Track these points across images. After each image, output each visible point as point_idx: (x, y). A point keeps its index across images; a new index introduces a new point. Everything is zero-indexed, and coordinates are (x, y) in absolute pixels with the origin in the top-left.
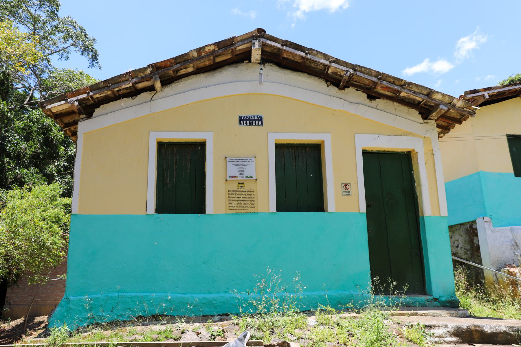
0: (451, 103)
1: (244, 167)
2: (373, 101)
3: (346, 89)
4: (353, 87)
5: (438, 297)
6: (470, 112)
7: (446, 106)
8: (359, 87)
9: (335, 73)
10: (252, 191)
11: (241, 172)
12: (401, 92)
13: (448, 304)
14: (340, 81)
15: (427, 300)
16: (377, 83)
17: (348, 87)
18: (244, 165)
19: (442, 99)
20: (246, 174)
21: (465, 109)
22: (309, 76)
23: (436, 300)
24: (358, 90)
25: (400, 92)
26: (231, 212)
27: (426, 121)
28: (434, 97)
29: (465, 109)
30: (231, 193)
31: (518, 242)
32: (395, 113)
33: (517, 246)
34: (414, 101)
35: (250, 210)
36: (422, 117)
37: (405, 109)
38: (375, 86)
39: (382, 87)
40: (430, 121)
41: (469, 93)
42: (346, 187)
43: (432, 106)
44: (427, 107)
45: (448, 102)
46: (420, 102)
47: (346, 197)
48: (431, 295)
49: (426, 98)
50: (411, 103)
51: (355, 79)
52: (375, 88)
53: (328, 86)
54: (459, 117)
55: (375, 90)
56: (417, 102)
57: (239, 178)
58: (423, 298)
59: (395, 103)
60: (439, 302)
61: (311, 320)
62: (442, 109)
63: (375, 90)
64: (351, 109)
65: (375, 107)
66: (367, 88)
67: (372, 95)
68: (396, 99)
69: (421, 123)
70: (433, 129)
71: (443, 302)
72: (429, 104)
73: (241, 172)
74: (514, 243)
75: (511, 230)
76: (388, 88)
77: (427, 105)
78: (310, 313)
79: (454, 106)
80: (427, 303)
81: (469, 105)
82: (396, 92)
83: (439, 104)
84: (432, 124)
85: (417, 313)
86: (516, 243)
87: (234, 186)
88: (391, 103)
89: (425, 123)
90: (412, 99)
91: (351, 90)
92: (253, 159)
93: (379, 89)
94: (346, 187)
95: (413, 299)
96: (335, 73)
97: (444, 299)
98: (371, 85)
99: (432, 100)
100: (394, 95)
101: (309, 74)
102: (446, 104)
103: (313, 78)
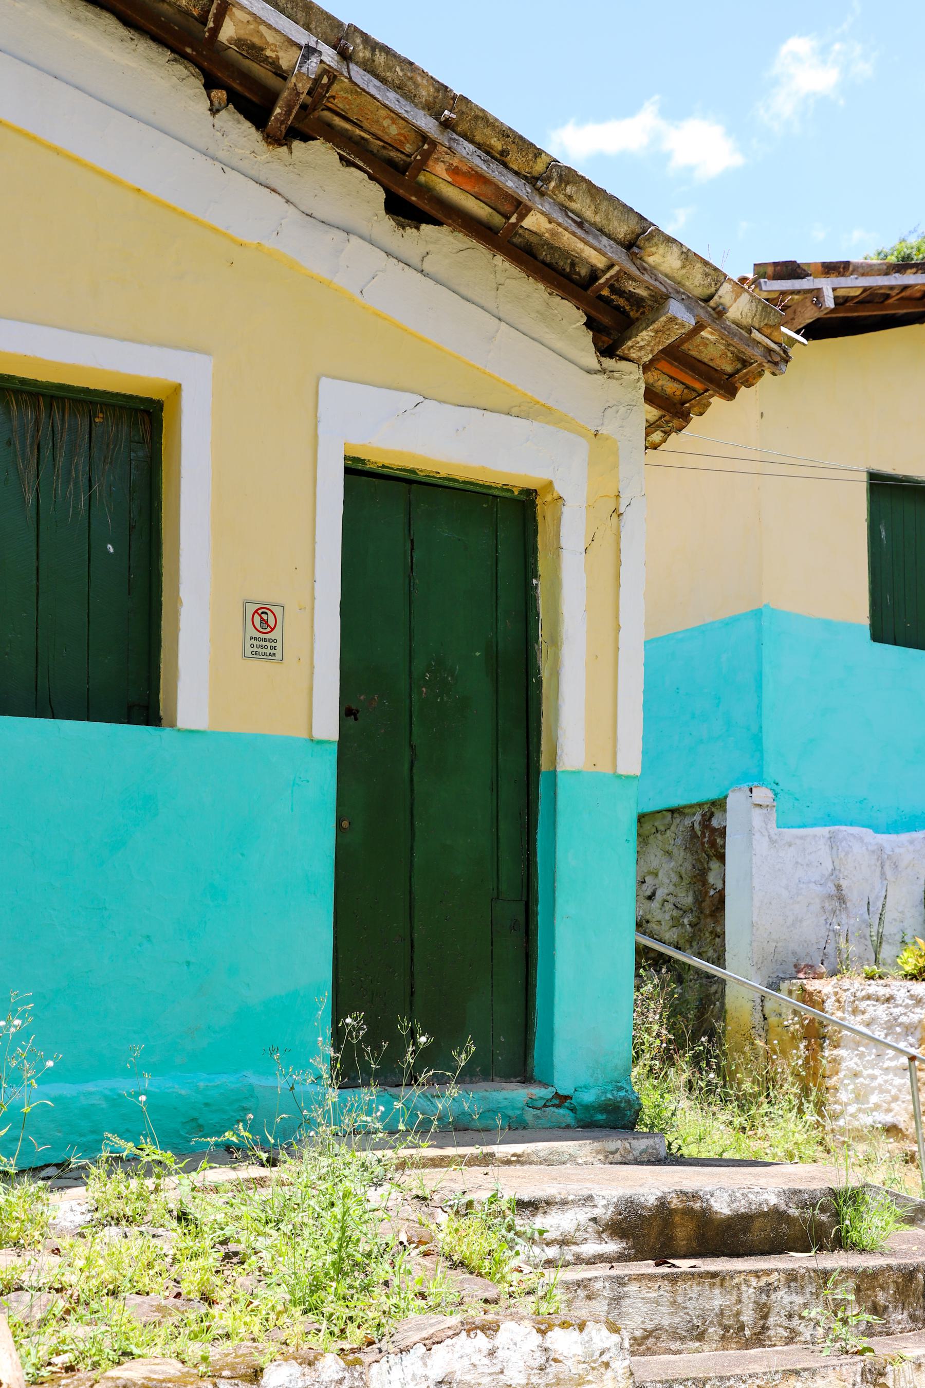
0: (711, 297)
2: (411, 232)
3: (297, 144)
4: (328, 140)
6: (770, 350)
7: (690, 309)
8: (358, 151)
9: (254, 51)
12: (529, 210)
13: (600, 1117)
14: (272, 97)
15: (531, 1104)
16: (434, 144)
17: (306, 138)
19: (679, 275)
21: (756, 335)
22: (123, 31)
23: (562, 1099)
24: (350, 164)
25: (522, 208)
27: (609, 363)
28: (651, 260)
29: (756, 335)
31: (844, 884)
32: (491, 305)
33: (842, 899)
34: (573, 265)
36: (595, 342)
37: (535, 292)
38: (427, 156)
39: (454, 171)
40: (623, 365)
41: (770, 270)
43: (636, 301)
44: (621, 302)
45: (698, 292)
46: (594, 275)
48: (546, 1085)
49: (619, 256)
50: (561, 273)
51: (339, 104)
52: (422, 166)
53: (214, 111)
54: (729, 369)
55: (422, 178)
56: (584, 271)
58: (515, 1095)
59: (499, 258)
60: (573, 1110)
61: (68, 1207)
62: (673, 320)
63: (422, 178)
64: (312, 252)
65: (415, 261)
66: (390, 162)
67: (410, 206)
68: (503, 238)
69: (589, 372)
70: (631, 406)
71: (587, 1108)
72: (630, 286)
74: (833, 891)
75: (832, 840)
76: (479, 177)
77: (621, 293)
78: (61, 1173)
79: (720, 313)
80: (530, 1115)
81: (773, 320)
82: (507, 208)
83: (667, 297)
84: (629, 380)
85: (492, 1155)
86: (839, 887)
88: (481, 252)
89: (603, 371)
90: (565, 254)
91: (318, 153)
93: (438, 178)
95: (484, 1099)
96: (253, 46)
97: (588, 1097)
98: (408, 148)
99: (643, 270)
100: (498, 220)
101: (127, 22)
102: (690, 301)
103: (144, 47)
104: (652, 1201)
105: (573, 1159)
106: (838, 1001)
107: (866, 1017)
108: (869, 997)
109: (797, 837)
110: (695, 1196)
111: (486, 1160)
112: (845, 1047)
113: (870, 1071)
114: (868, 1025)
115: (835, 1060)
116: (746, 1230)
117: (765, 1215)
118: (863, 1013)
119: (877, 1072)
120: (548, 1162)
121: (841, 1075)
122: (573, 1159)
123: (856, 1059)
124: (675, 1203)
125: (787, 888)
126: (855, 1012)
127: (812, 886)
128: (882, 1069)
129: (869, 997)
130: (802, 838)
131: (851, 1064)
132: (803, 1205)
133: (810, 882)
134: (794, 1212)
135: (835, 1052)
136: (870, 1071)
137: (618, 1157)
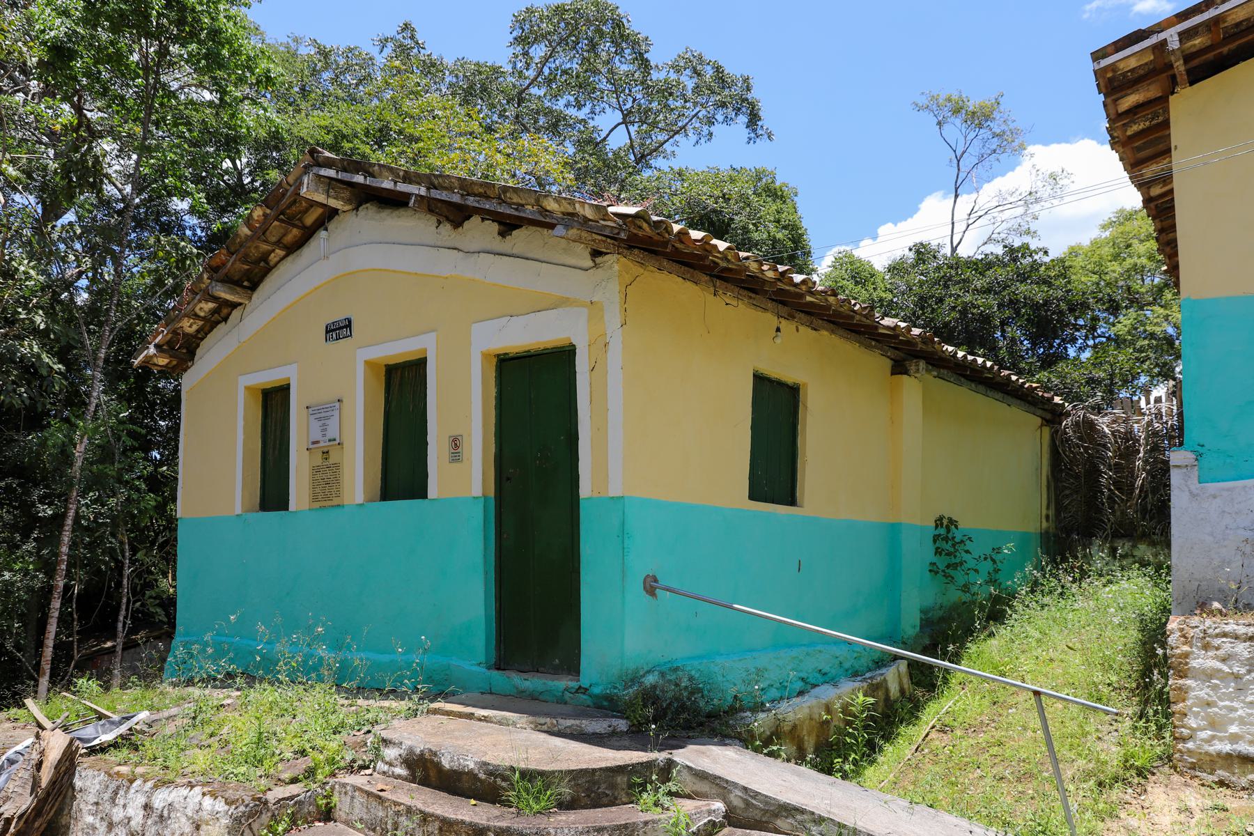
1: (327, 422)
5: (587, 686)
8: (487, 215)
10: (337, 466)
11: (324, 430)
13: (605, 703)
18: (327, 418)
20: (330, 435)
26: (317, 505)
30: (316, 470)
35: (336, 501)
42: (456, 443)
47: (454, 465)
57: (322, 444)
58: (562, 683)
71: (597, 696)
73: (324, 430)
80: (568, 695)
87: (318, 460)
92: (337, 404)
94: (456, 443)
97: (597, 690)
104: (418, 751)
105: (514, 724)
106: (1184, 636)
107: (1221, 652)
108: (1225, 635)
109: (1223, 489)
110: (435, 754)
111: (470, 716)
112: (1193, 678)
113: (1227, 703)
114: (1224, 660)
115: (1180, 689)
116: (459, 780)
117: (465, 773)
118: (1218, 649)
119: (1235, 704)
120: (500, 723)
121: (1189, 703)
122: (514, 724)
123: (1208, 690)
124: (427, 756)
125: (1211, 534)
126: (1206, 647)
127: (1241, 532)
128: (1243, 702)
129: (1225, 635)
130: (1228, 490)
131: (1202, 694)
132: (490, 774)
133: (1238, 528)
134: (482, 776)
135: (1181, 682)
136: (1227, 703)
137: (545, 728)
